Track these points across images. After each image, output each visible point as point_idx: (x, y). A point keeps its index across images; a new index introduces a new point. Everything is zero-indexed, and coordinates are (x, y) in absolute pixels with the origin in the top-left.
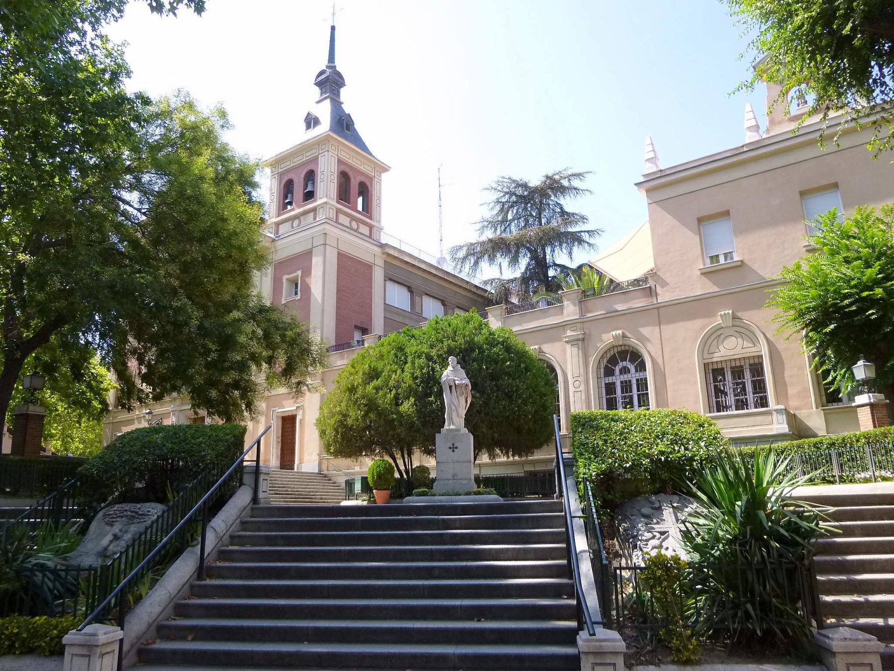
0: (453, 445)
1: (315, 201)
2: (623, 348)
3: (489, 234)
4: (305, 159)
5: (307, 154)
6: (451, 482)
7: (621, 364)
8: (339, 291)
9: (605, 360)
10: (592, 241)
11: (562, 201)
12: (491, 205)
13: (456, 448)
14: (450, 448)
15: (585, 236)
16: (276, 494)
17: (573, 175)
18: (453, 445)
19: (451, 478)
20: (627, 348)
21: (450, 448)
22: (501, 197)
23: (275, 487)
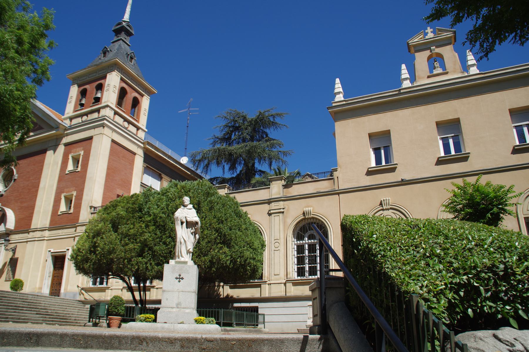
0: (180, 275)
1: (101, 104)
2: (312, 220)
3: (218, 146)
4: (97, 75)
5: (100, 72)
6: (174, 310)
7: (309, 232)
8: (108, 168)
9: (298, 228)
10: (285, 159)
11: (267, 131)
12: (222, 128)
13: (182, 279)
14: (177, 278)
15: (281, 156)
16: (37, 314)
17: (277, 115)
18: (180, 275)
19: (175, 306)
20: (315, 220)
21: (177, 278)
22: (229, 123)
23: (38, 308)
